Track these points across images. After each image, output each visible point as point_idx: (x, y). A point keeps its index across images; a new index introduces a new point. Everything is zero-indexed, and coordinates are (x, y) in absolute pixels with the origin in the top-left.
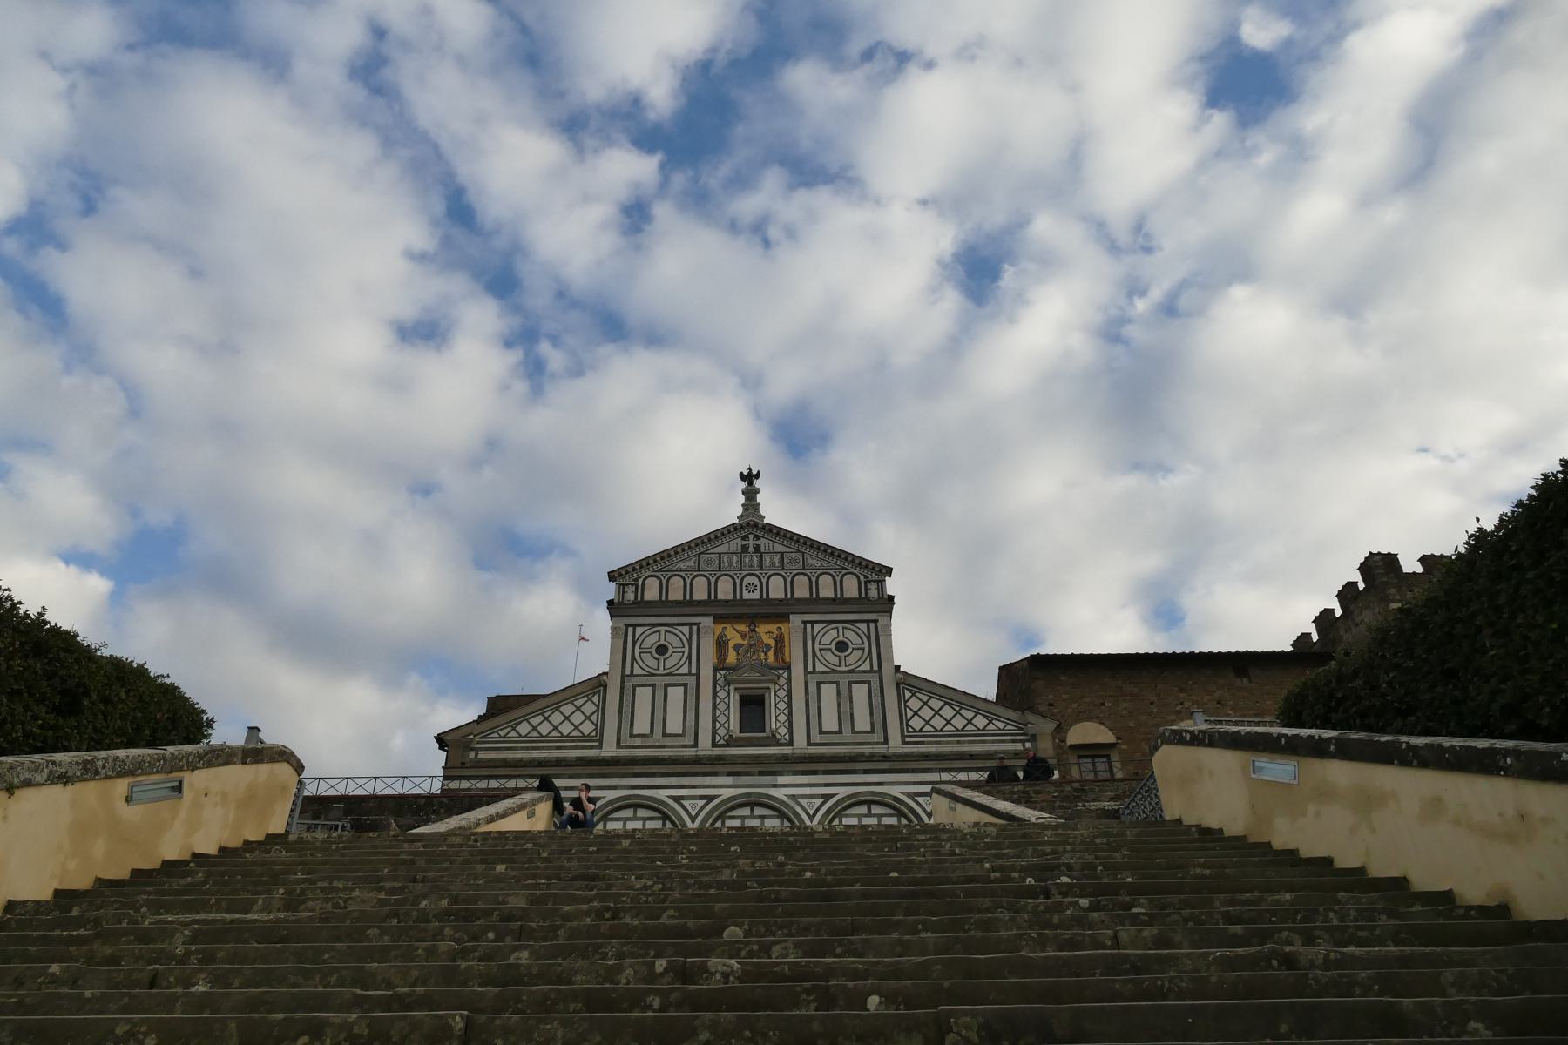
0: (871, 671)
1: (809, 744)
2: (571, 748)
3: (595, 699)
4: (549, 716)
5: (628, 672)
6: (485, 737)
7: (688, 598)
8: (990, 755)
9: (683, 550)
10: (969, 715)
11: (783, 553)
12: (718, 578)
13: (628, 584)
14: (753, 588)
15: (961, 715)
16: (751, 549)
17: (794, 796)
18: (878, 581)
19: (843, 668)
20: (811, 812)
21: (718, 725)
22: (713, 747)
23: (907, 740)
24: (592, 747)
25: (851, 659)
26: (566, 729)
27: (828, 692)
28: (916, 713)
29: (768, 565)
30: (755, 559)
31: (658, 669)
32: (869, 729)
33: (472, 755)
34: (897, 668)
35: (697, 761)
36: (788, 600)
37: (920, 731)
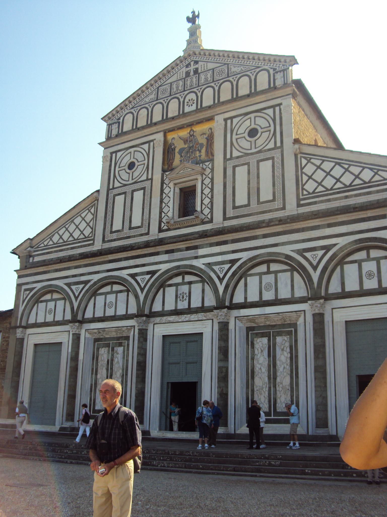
0: (275, 148)
1: (225, 219)
2: (79, 247)
3: (92, 210)
4: (68, 227)
5: (111, 187)
6: (38, 247)
8: (373, 204)
9: (147, 88)
10: (356, 170)
11: (213, 69)
13: (113, 123)
15: (349, 172)
16: (192, 73)
17: (209, 264)
18: (283, 71)
19: (254, 150)
20: (221, 276)
23: (302, 202)
24: (89, 245)
25: (259, 142)
26: (76, 234)
27: (242, 172)
28: (310, 177)
29: (202, 81)
30: (194, 80)
31: (129, 181)
32: (271, 198)
33: (31, 259)
34: (297, 141)
35: (147, 245)
37: (314, 192)
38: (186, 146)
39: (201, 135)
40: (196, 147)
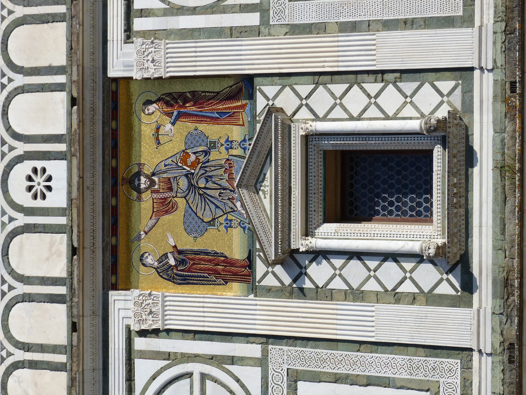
7: (62, 358)
12: (12, 272)
14: (39, 179)
21: (408, 287)
22: (470, 305)
36: (72, 82)
38: (181, 203)
39: (159, 143)
40: (193, 165)
